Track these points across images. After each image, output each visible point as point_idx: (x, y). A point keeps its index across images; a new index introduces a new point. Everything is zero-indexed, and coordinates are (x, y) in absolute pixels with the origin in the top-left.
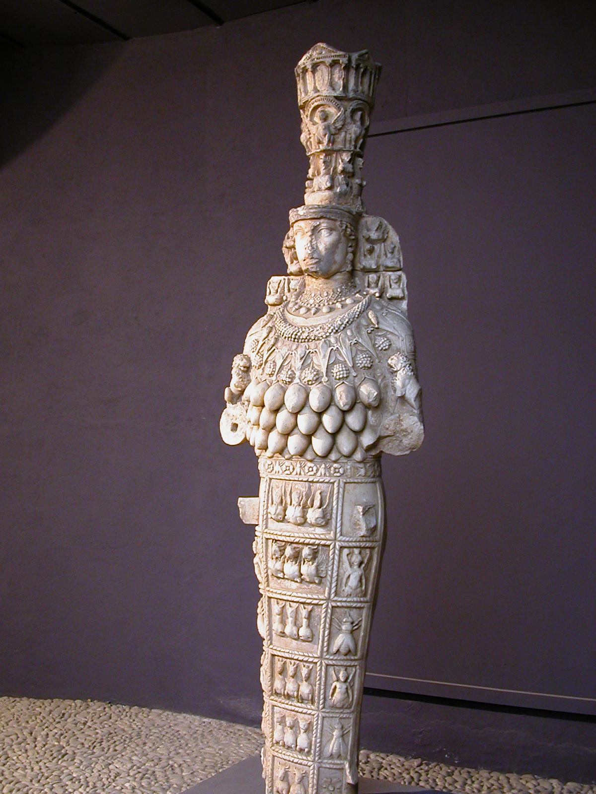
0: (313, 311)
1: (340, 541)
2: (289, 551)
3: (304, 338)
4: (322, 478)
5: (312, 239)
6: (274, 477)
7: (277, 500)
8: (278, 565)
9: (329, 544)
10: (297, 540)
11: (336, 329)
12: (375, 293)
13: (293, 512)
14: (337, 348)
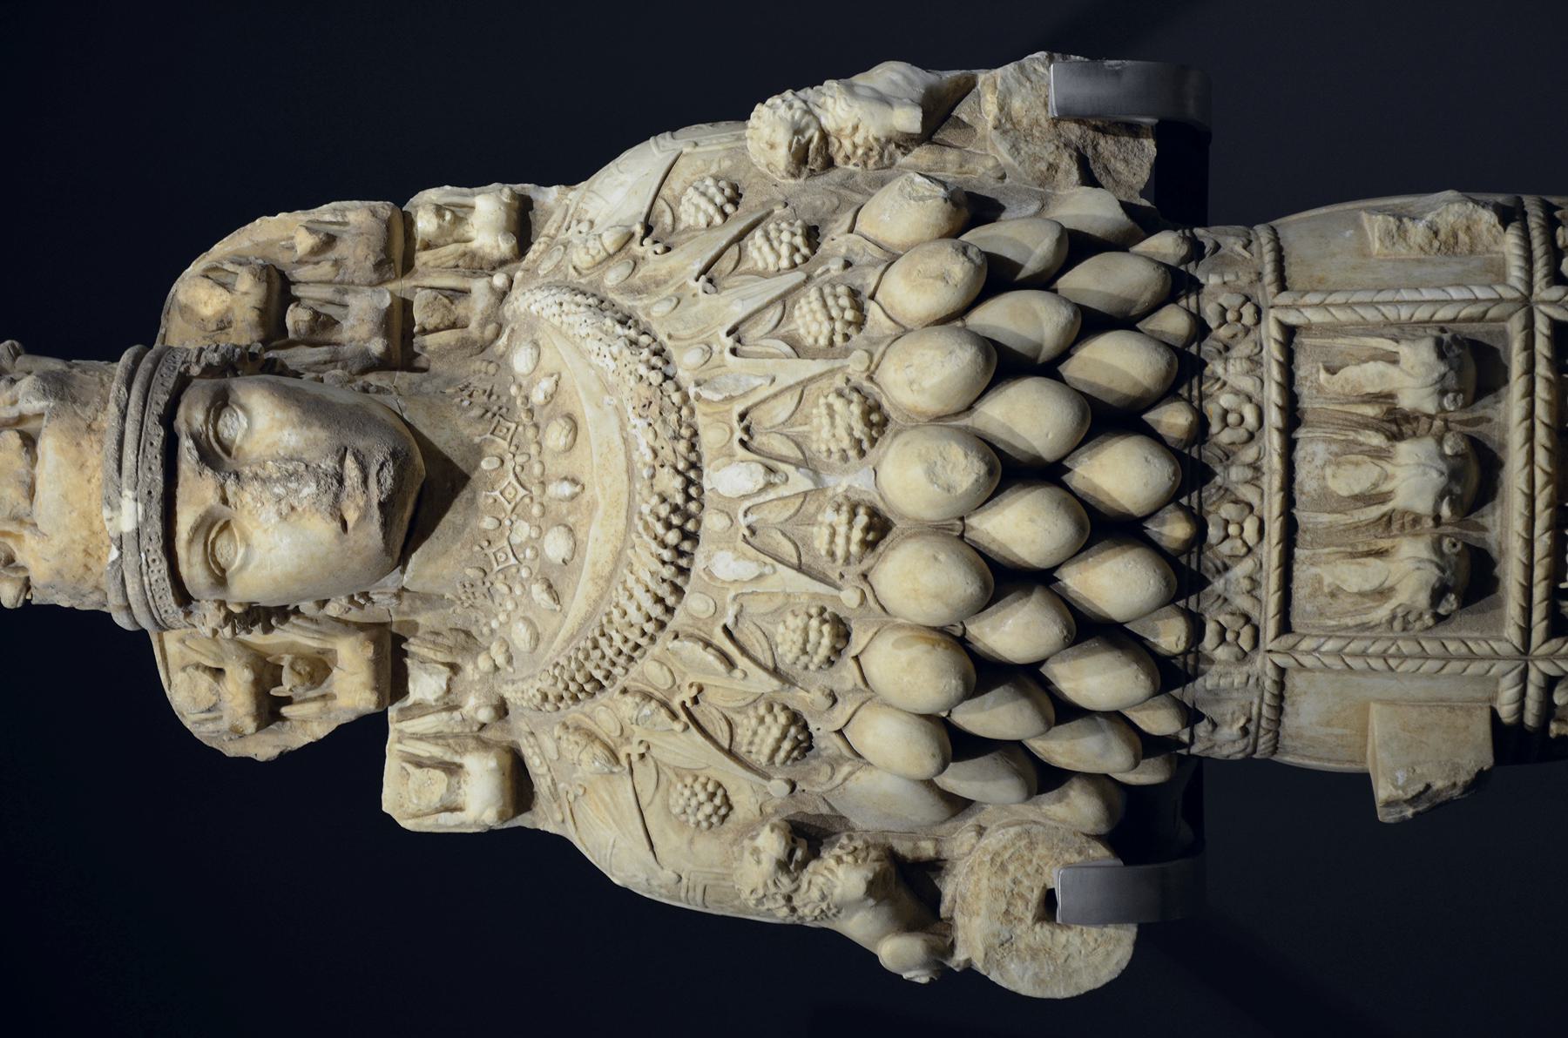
1: (1530, 285)
3: (678, 482)
4: (1269, 371)
5: (256, 477)
9: (1546, 321)
11: (646, 353)
12: (492, 288)
14: (729, 334)
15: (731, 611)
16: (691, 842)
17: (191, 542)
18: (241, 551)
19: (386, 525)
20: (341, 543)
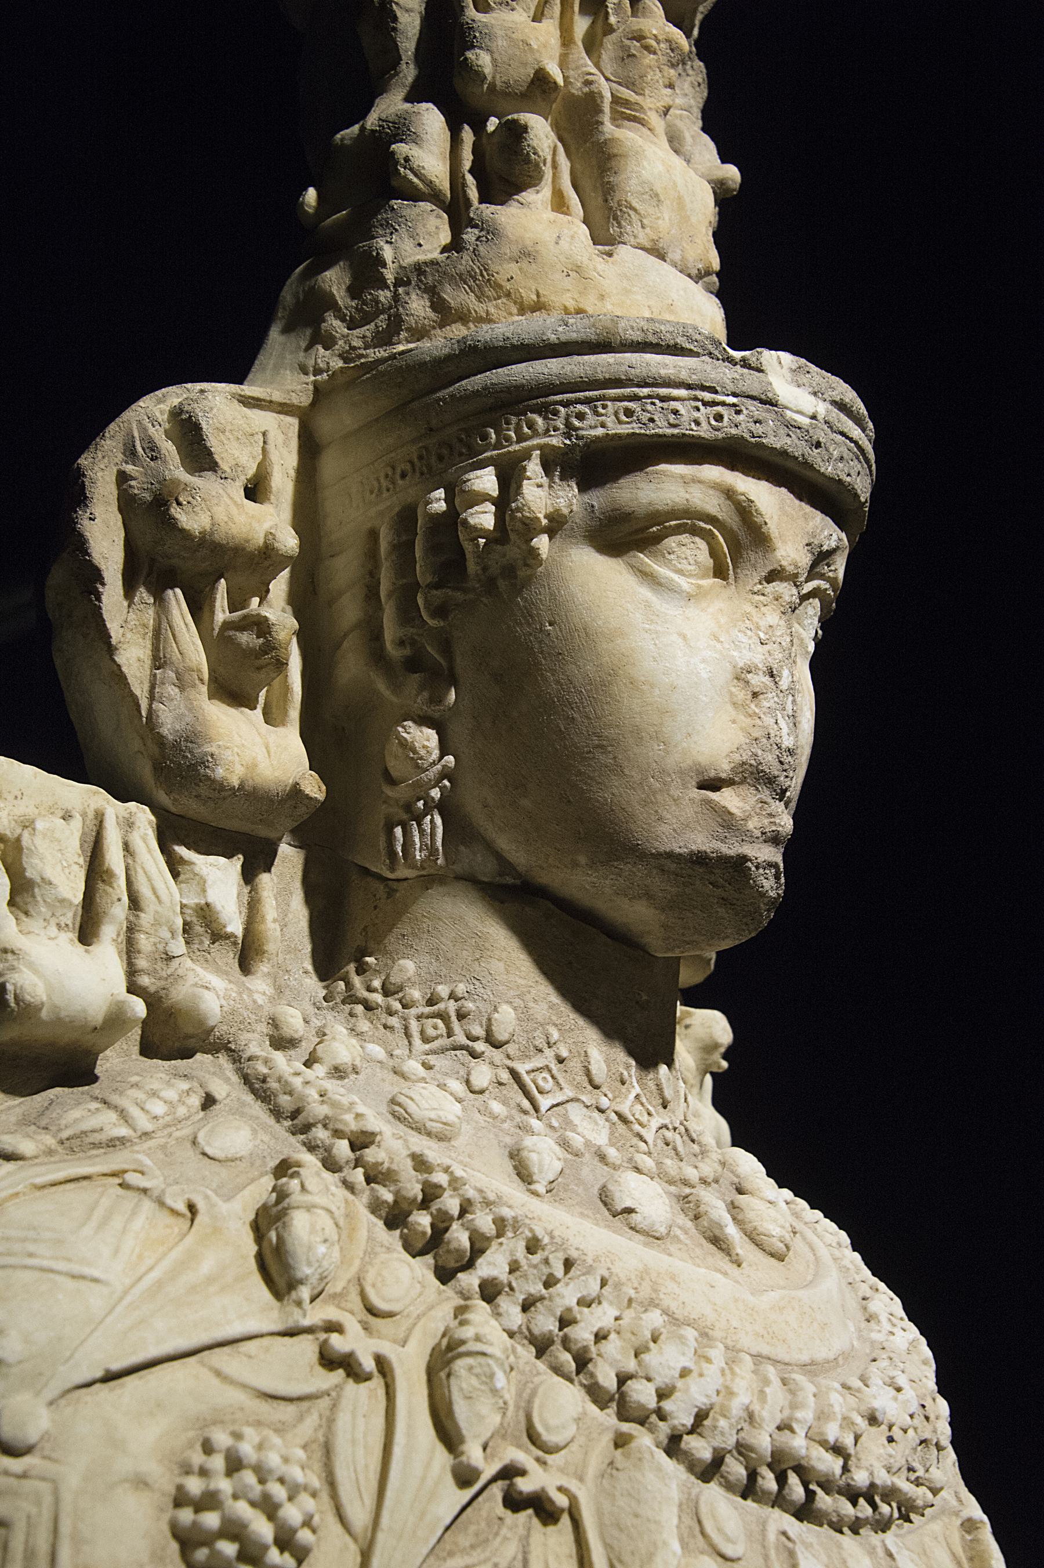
16: (141, 1483)
17: (729, 494)
18: (684, 583)
19: (699, 859)
20: (681, 773)
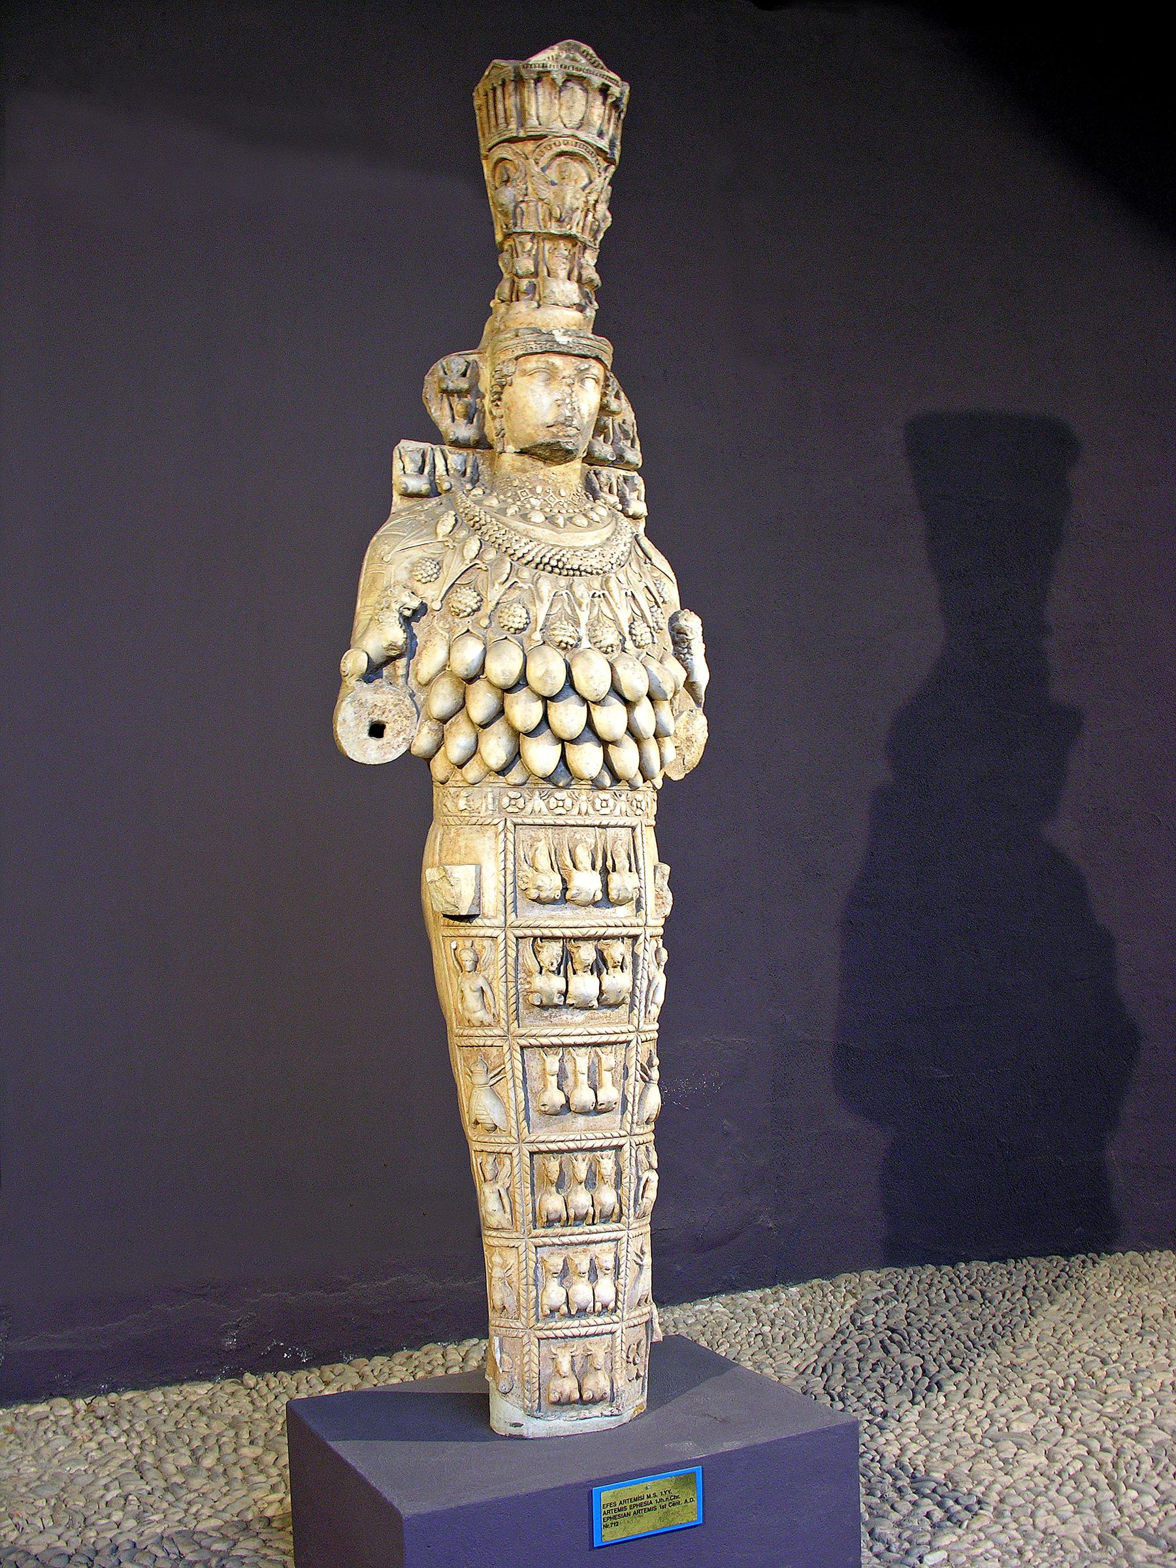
0: (561, 521)
2: (586, 953)
6: (527, 821)
7: (543, 862)
8: (558, 983)
10: (592, 932)
13: (587, 882)
15: (526, 587)
